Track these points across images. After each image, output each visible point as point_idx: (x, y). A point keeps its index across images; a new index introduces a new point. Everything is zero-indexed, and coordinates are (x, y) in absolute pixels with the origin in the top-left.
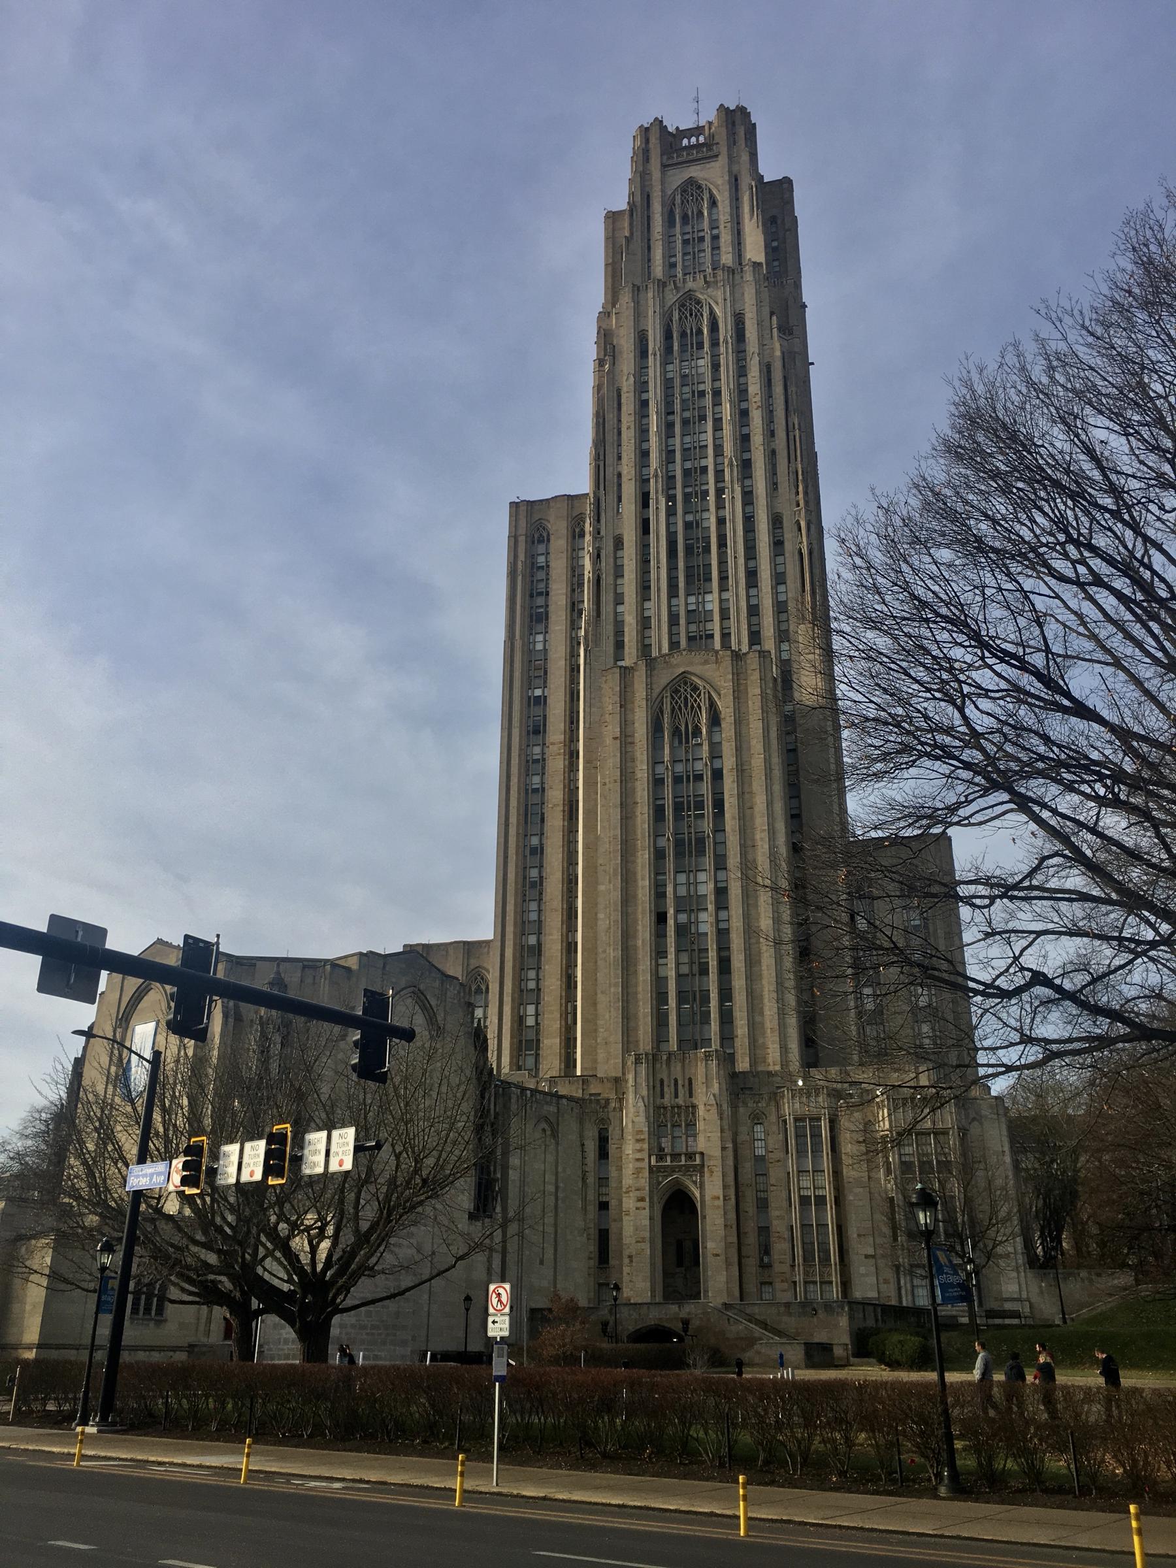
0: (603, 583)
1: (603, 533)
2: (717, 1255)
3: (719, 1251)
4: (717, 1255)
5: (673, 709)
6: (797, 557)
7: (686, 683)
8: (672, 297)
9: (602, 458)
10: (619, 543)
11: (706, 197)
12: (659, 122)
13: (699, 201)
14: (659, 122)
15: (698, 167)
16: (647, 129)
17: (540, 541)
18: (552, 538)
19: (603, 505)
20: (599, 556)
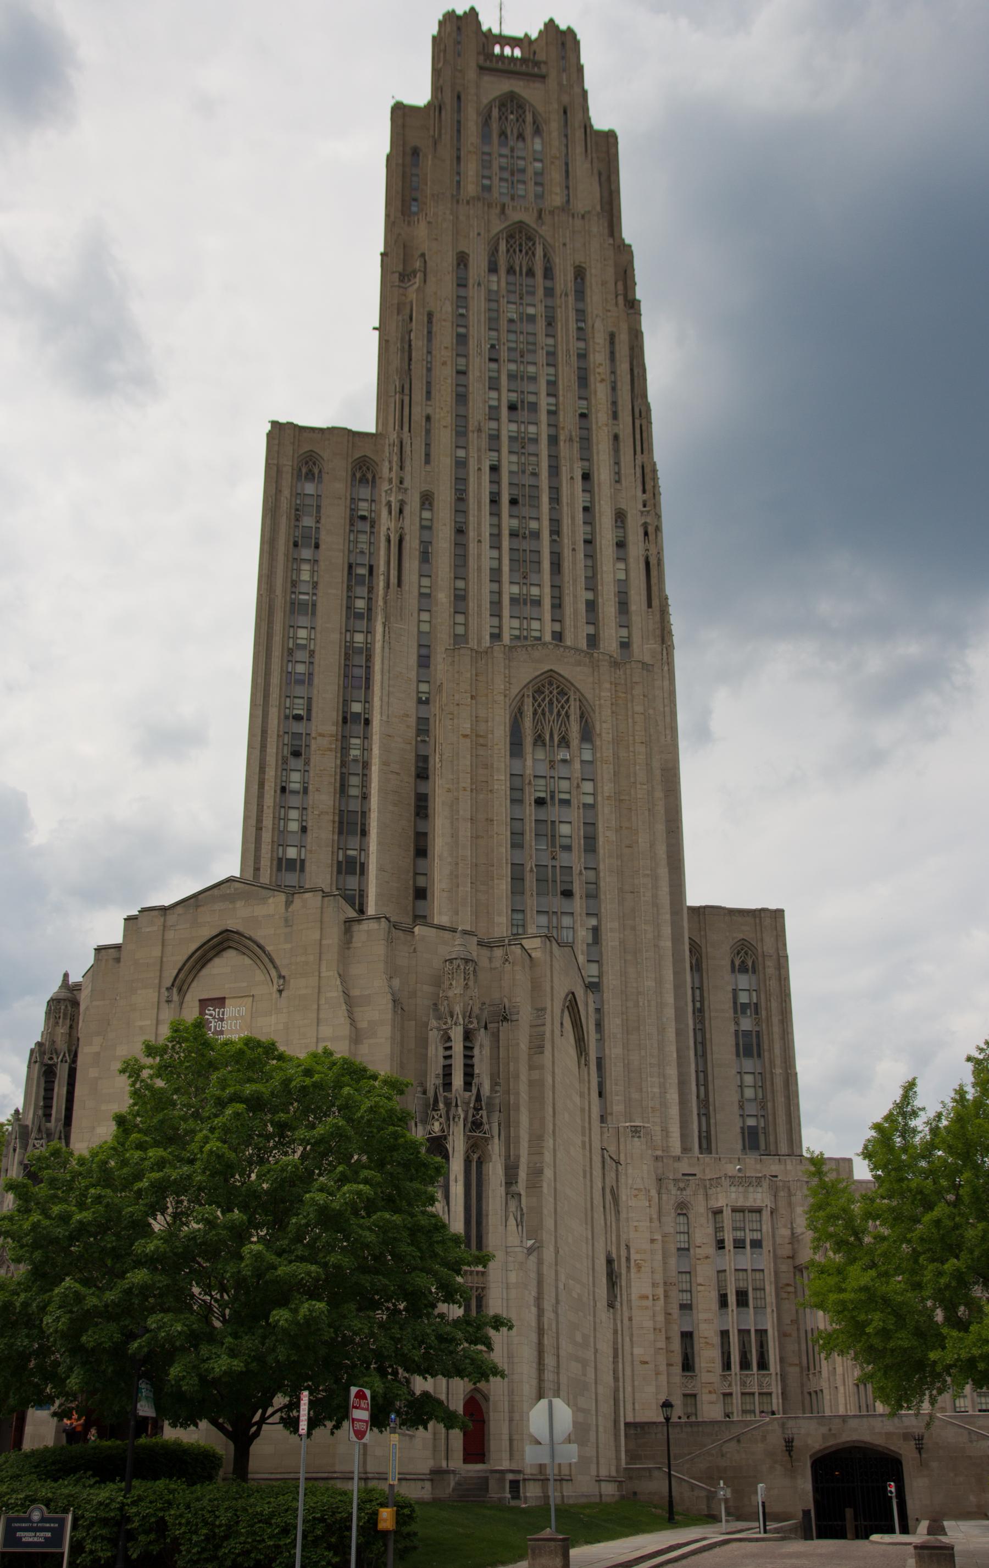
0: (406, 545)
1: (407, 484)
2: (646, 1363)
3: (647, 1359)
4: (646, 1363)
5: (535, 713)
6: (642, 566)
7: (551, 684)
8: (498, 226)
9: (407, 391)
10: (427, 500)
11: (529, 118)
12: (473, 14)
13: (521, 119)
14: (473, 14)
16: (459, 18)
17: (310, 476)
18: (325, 476)
19: (407, 448)
20: (401, 511)
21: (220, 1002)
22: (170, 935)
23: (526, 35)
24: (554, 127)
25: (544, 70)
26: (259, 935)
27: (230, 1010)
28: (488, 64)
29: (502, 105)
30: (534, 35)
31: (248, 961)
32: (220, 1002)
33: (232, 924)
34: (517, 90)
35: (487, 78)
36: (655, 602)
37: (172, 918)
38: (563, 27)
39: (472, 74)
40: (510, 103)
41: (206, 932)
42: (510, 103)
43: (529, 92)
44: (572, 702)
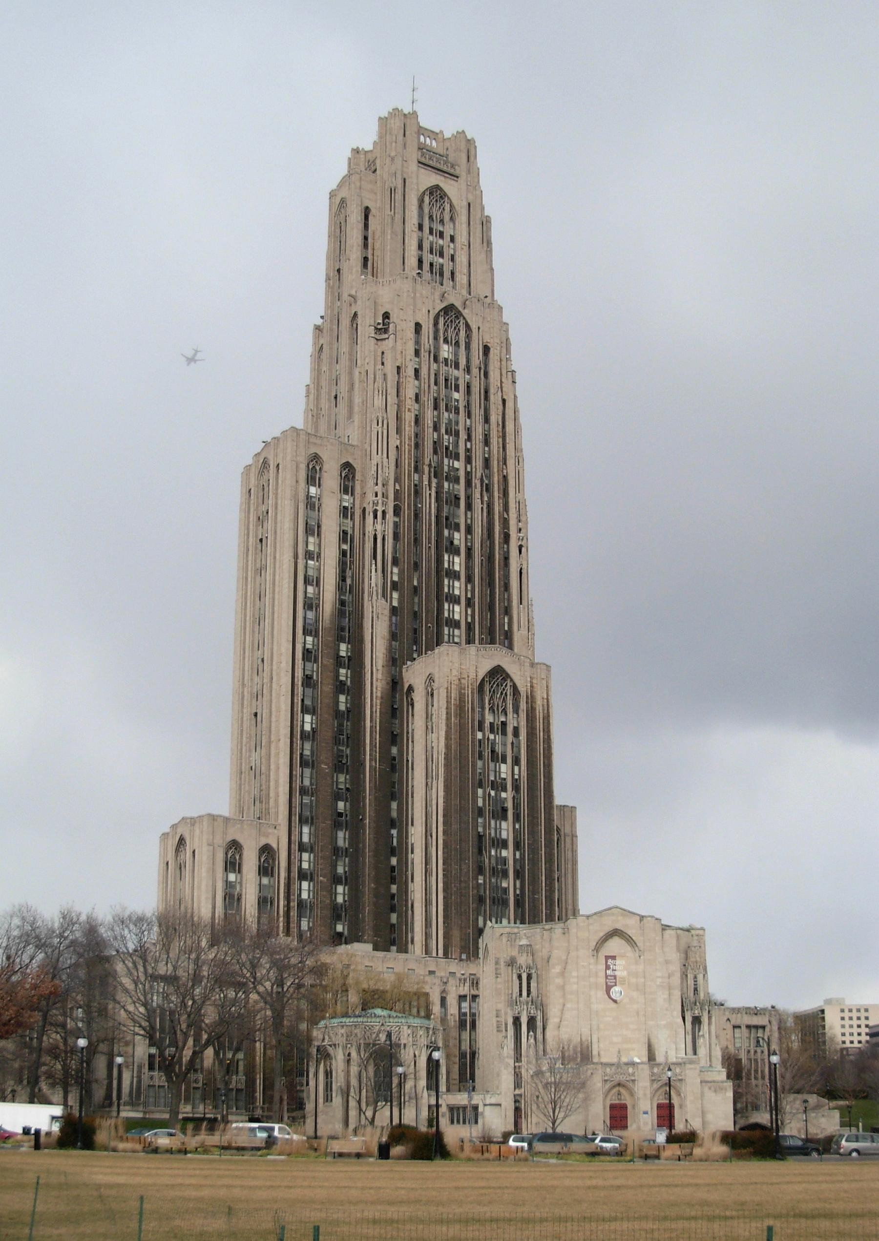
11: (447, 208)
15: (443, 178)
21: (614, 958)
22: (591, 927)
23: (441, 132)
24: (462, 218)
25: (457, 172)
26: (630, 933)
27: (618, 962)
28: (423, 160)
29: (431, 194)
30: (447, 135)
31: (623, 942)
32: (614, 958)
33: (618, 926)
34: (442, 185)
35: (422, 171)
36: (524, 601)
37: (591, 920)
38: (469, 137)
39: (413, 166)
40: (436, 193)
41: (608, 928)
42: (436, 193)
43: (449, 187)
44: (508, 687)
